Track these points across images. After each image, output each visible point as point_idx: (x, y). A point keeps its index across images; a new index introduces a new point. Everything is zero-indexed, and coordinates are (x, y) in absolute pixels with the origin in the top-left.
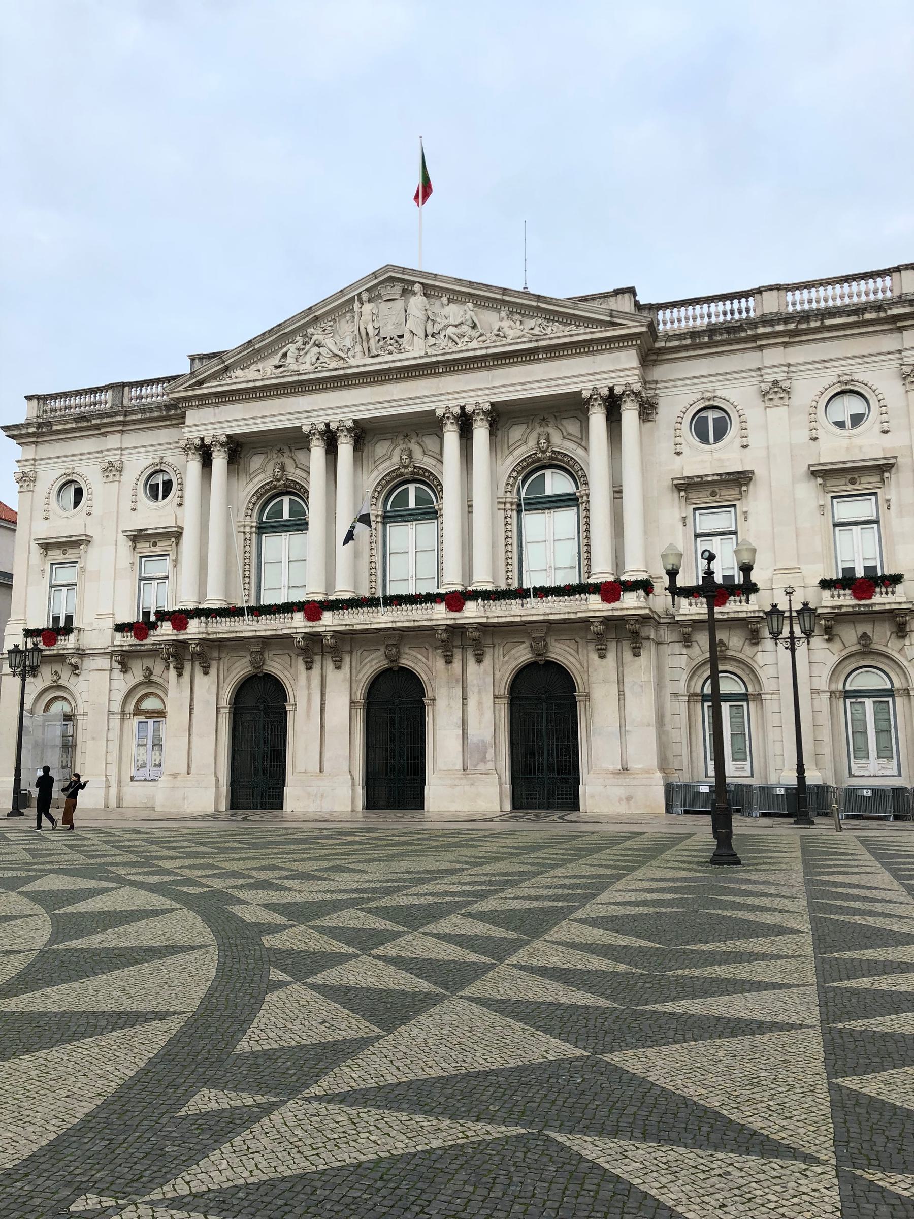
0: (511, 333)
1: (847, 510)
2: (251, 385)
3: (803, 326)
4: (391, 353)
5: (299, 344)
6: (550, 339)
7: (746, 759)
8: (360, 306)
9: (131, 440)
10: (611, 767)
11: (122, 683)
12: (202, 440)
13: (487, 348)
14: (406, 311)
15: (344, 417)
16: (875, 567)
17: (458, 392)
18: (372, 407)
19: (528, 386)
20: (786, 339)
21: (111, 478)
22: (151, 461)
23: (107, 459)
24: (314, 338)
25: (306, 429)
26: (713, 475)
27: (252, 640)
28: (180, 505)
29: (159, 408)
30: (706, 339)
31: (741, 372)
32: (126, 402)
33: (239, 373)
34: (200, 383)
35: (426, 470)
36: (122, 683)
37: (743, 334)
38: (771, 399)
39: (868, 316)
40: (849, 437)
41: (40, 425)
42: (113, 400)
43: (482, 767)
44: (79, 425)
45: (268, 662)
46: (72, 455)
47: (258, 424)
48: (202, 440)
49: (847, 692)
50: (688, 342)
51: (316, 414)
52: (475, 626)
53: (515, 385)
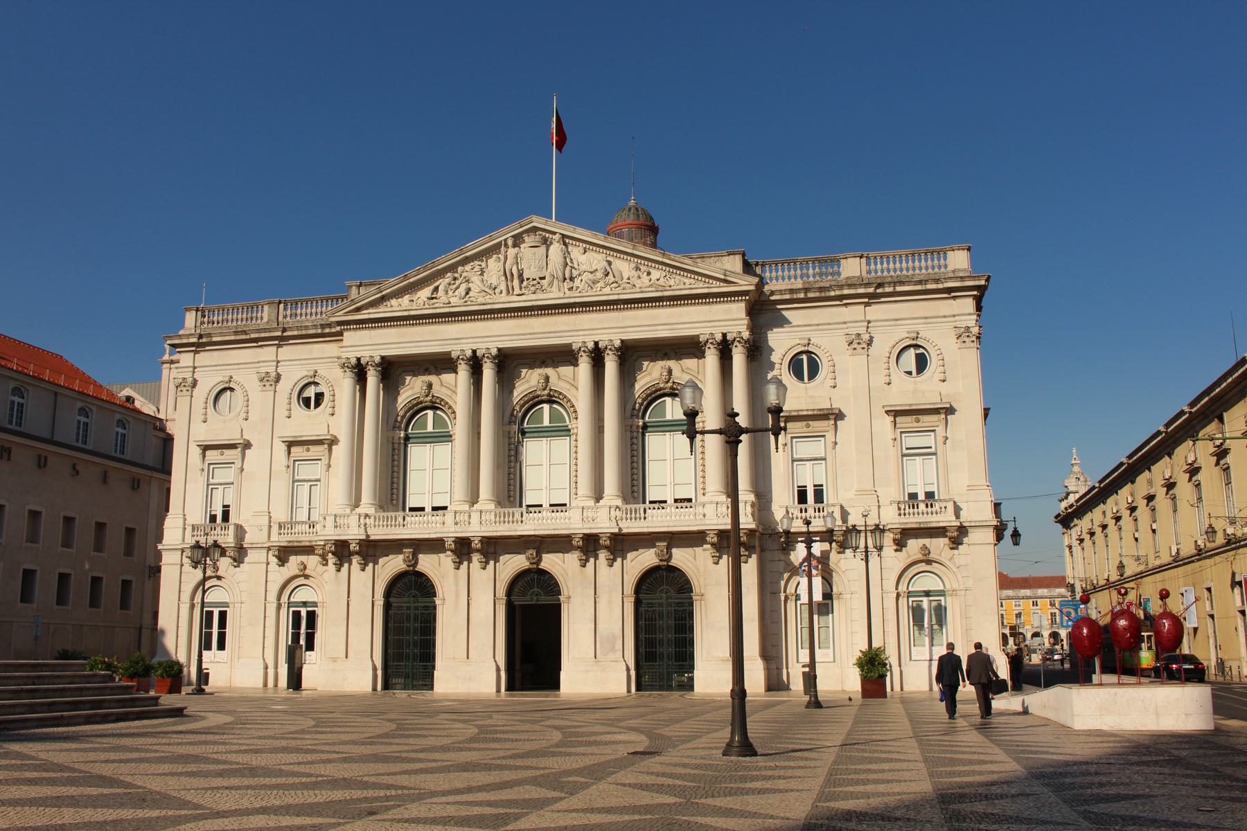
0: (638, 283)
1: (912, 441)
2: (406, 313)
3: (879, 291)
4: (534, 293)
6: (673, 290)
7: (829, 648)
9: (287, 352)
10: (721, 655)
11: (279, 575)
12: (359, 359)
13: (619, 294)
14: (547, 257)
15: (490, 345)
16: (933, 492)
17: (593, 329)
18: (514, 338)
19: (654, 328)
20: (866, 300)
21: (268, 387)
23: (264, 370)
25: (454, 355)
26: (808, 410)
28: (333, 415)
29: (315, 326)
30: (802, 296)
31: (830, 324)
32: (281, 318)
33: (394, 302)
34: (358, 310)
35: (561, 393)
36: (279, 575)
37: (832, 294)
38: (855, 349)
39: (930, 286)
40: (915, 383)
41: (201, 336)
42: (269, 316)
43: (611, 656)
44: (238, 337)
45: (420, 562)
46: (231, 365)
47: (410, 347)
49: (909, 592)
50: (787, 297)
51: (464, 341)
52: (608, 535)
53: (643, 326)
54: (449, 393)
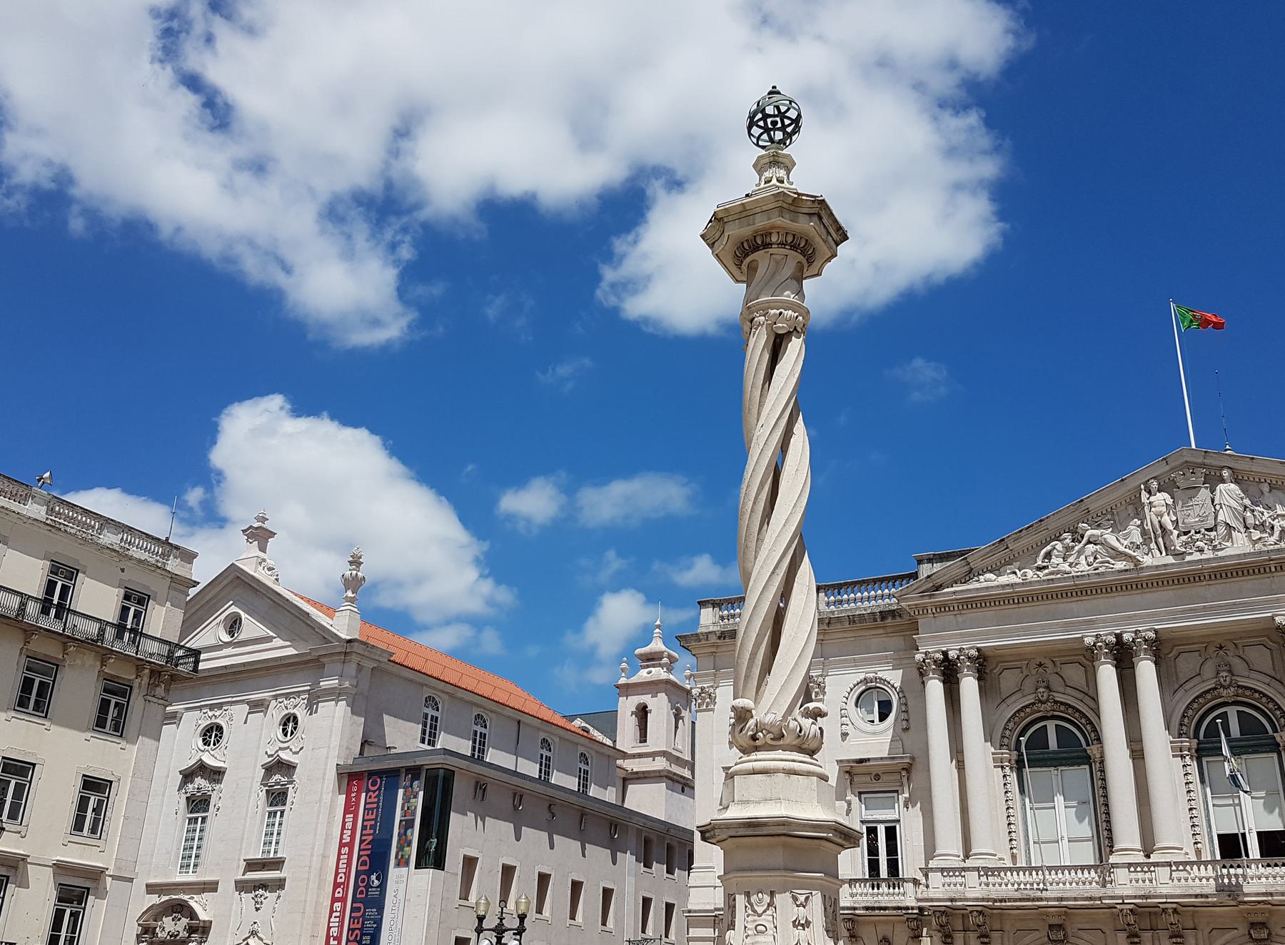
5: (1068, 541)
8: (1148, 496)
12: (945, 654)
14: (1213, 502)
22: (862, 676)
24: (1088, 533)
27: (1050, 909)
28: (907, 729)
48: (945, 654)
54: (1080, 696)
